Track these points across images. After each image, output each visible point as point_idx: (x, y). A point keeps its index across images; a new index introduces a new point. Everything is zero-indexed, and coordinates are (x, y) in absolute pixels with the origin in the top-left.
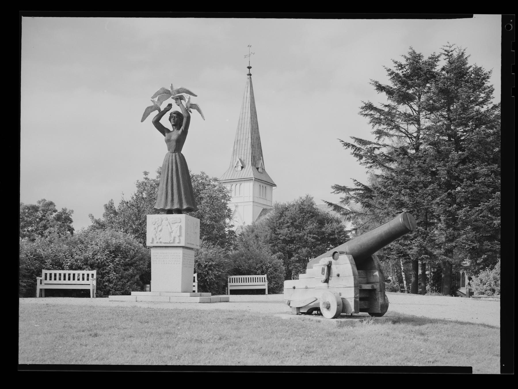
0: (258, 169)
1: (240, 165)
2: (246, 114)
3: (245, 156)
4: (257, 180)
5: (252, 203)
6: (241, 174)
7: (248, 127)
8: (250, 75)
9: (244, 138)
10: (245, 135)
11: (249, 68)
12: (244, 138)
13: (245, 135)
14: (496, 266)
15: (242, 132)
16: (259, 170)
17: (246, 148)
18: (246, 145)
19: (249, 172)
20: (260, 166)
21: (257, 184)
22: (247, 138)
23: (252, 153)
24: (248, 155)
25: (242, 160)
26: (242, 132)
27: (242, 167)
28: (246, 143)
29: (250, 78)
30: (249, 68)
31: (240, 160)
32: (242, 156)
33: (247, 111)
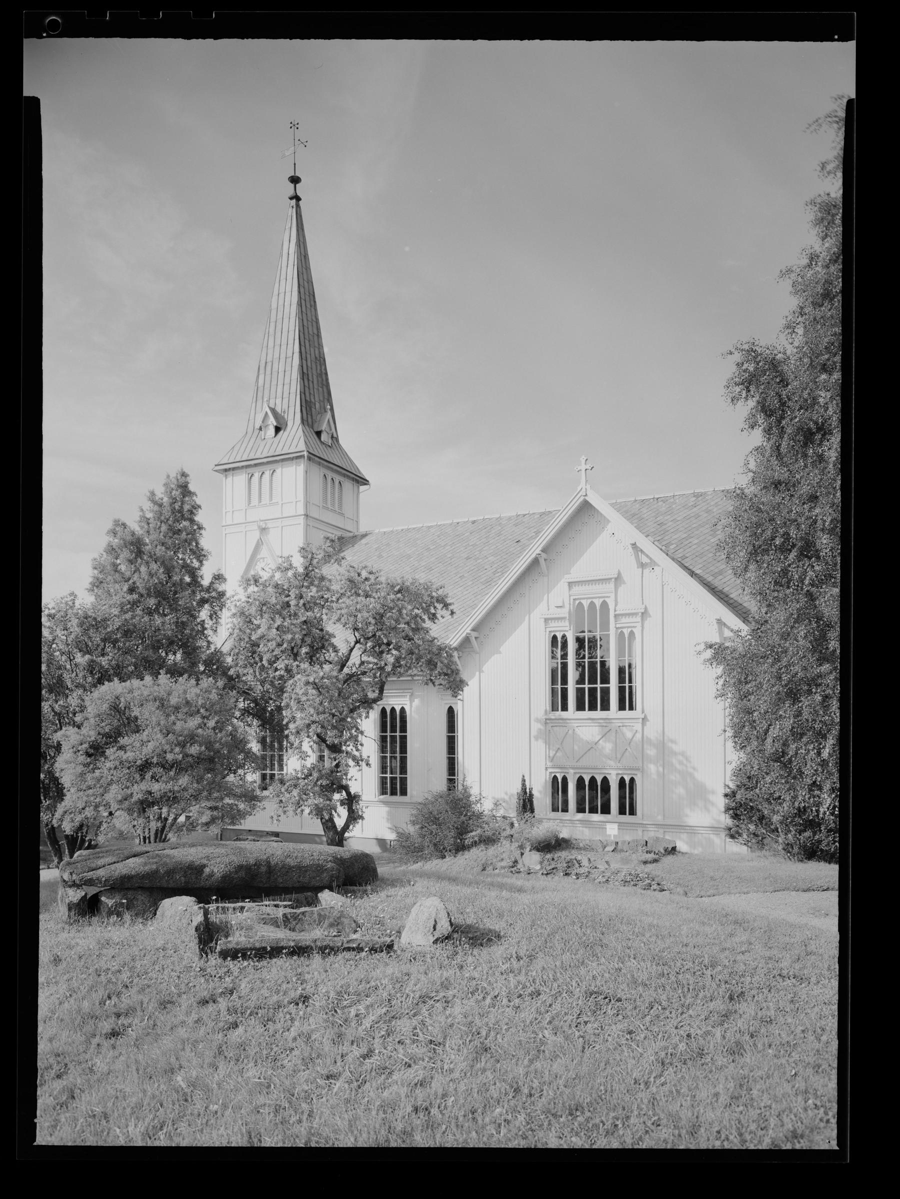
0: (319, 434)
1: (272, 421)
2: (288, 294)
3: (286, 401)
4: (312, 458)
5: (301, 520)
6: (275, 446)
7: (292, 328)
8: (297, 198)
9: (283, 356)
10: (284, 347)
11: (295, 180)
12: (283, 356)
13: (284, 347)
14: (242, 846)
15: (278, 342)
16: (324, 437)
17: (287, 381)
18: (288, 373)
19: (295, 437)
20: (324, 427)
21: (317, 473)
22: (290, 354)
23: (303, 393)
24: (293, 396)
25: (278, 409)
26: (278, 342)
27: (278, 429)
28: (288, 368)
29: (298, 206)
30: (295, 180)
31: (273, 411)
32: (279, 401)
33: (288, 289)
